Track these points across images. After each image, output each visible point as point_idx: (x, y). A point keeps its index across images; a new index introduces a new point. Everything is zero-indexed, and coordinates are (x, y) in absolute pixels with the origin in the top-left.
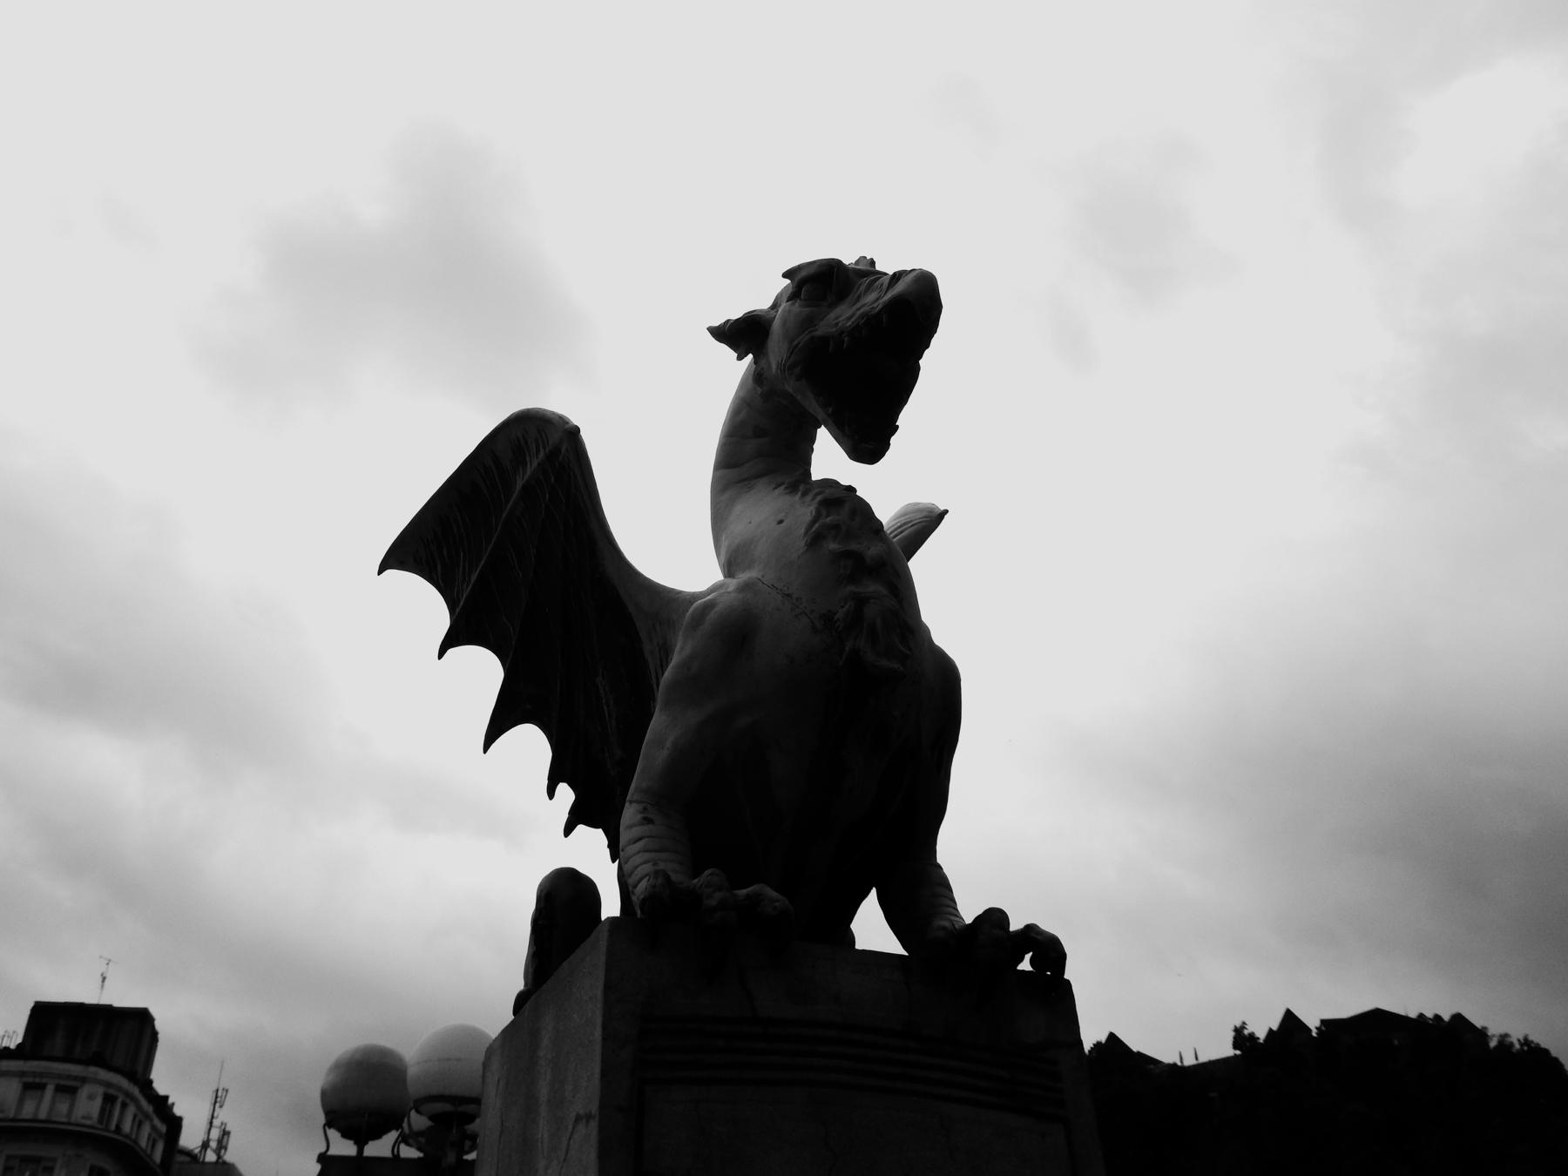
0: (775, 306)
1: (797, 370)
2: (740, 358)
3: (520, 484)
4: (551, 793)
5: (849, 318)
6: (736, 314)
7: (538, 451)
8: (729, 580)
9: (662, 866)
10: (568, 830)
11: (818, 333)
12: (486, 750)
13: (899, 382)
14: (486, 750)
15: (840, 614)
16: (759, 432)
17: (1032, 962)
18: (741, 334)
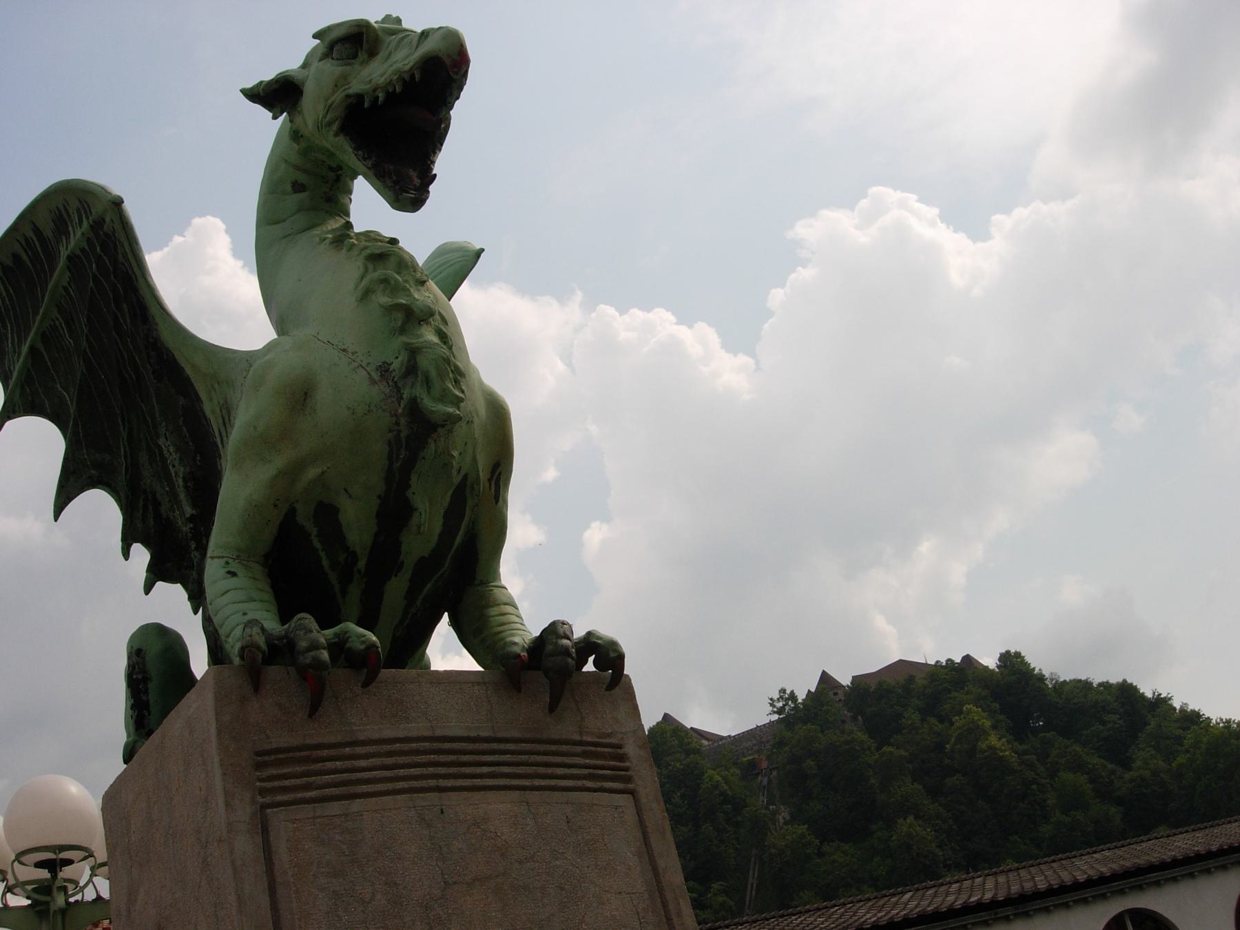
0: (305, 65)
1: (335, 127)
2: (275, 118)
3: (64, 253)
4: (126, 554)
5: (382, 76)
6: (269, 76)
7: (81, 222)
8: (285, 338)
9: (250, 616)
10: (148, 588)
11: (351, 91)
12: (56, 518)
13: (430, 135)
14: (57, 516)
15: (396, 365)
16: (298, 187)
18: (277, 95)
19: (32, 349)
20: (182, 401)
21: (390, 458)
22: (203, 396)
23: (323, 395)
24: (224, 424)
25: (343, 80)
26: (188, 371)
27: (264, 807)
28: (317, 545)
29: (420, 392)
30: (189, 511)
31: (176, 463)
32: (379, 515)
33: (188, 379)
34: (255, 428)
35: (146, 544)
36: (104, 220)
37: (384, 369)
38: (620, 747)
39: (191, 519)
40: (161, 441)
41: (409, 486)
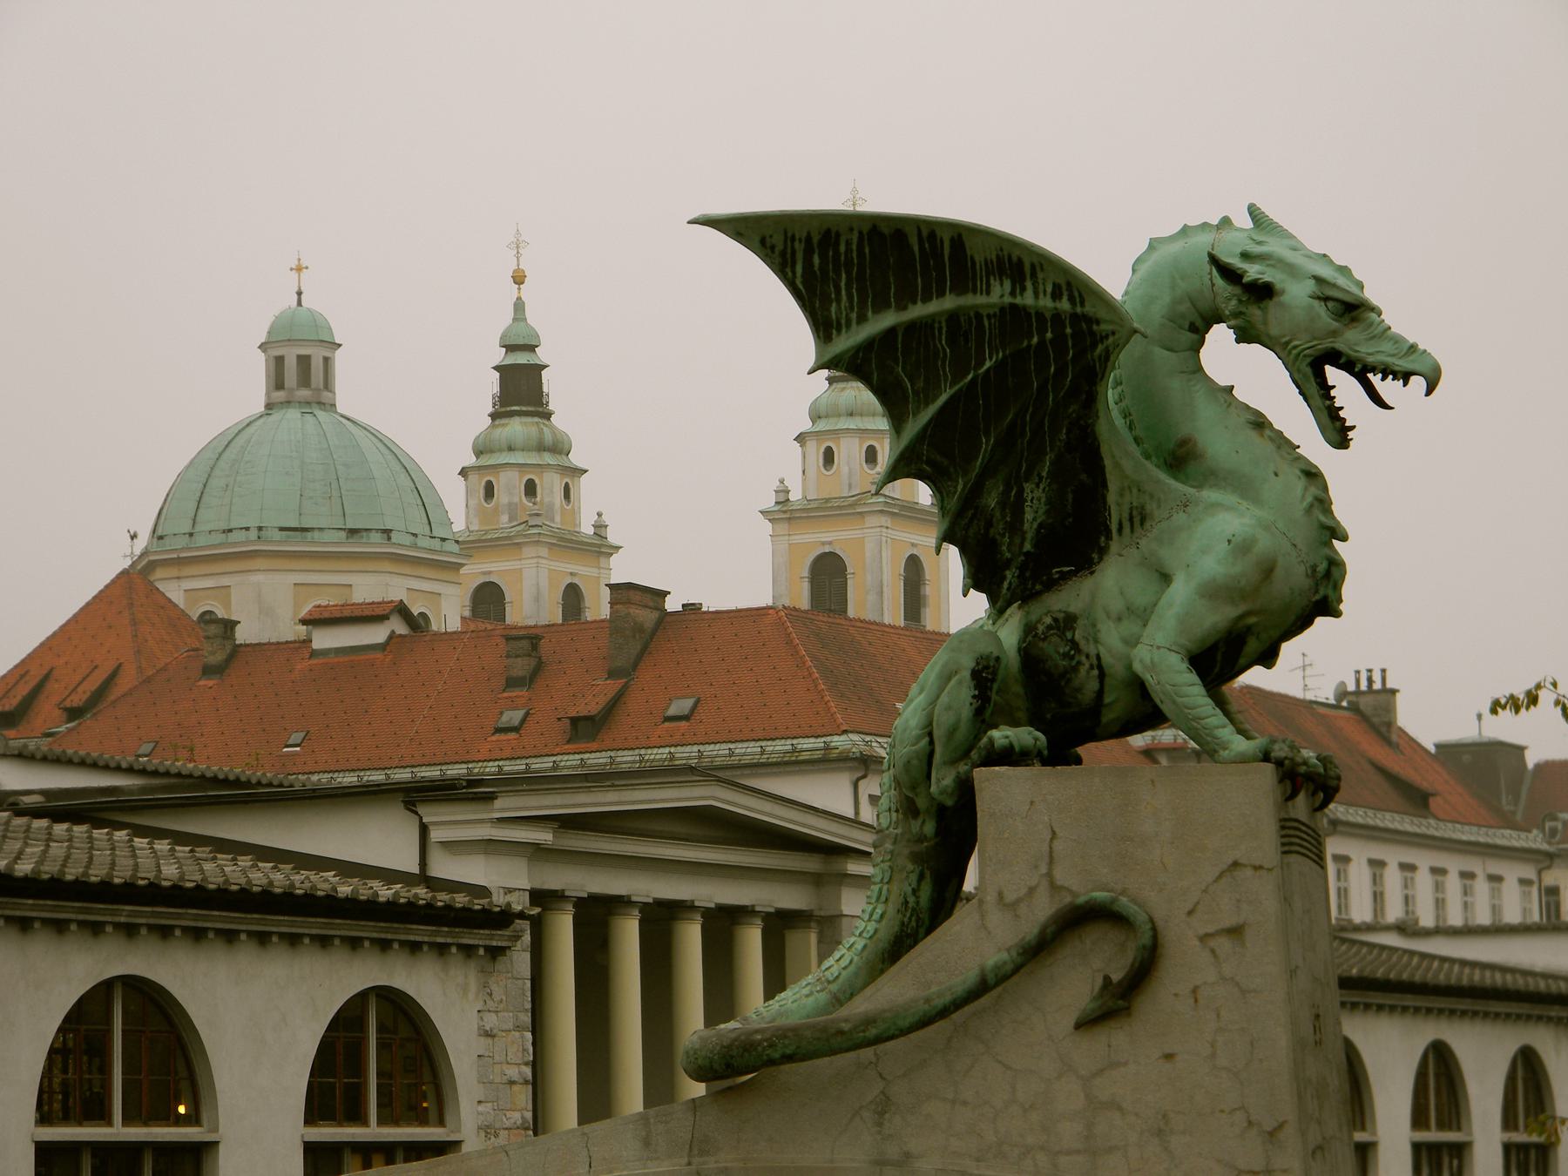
1: (1309, 360)
19: (891, 332)
20: (1084, 477)
22: (1113, 485)
23: (1279, 573)
24: (1131, 519)
25: (1334, 334)
26: (1108, 462)
29: (1330, 592)
30: (1028, 547)
31: (1041, 512)
35: (963, 552)
36: (1098, 322)
37: (1314, 568)
39: (1027, 554)
40: (1028, 487)
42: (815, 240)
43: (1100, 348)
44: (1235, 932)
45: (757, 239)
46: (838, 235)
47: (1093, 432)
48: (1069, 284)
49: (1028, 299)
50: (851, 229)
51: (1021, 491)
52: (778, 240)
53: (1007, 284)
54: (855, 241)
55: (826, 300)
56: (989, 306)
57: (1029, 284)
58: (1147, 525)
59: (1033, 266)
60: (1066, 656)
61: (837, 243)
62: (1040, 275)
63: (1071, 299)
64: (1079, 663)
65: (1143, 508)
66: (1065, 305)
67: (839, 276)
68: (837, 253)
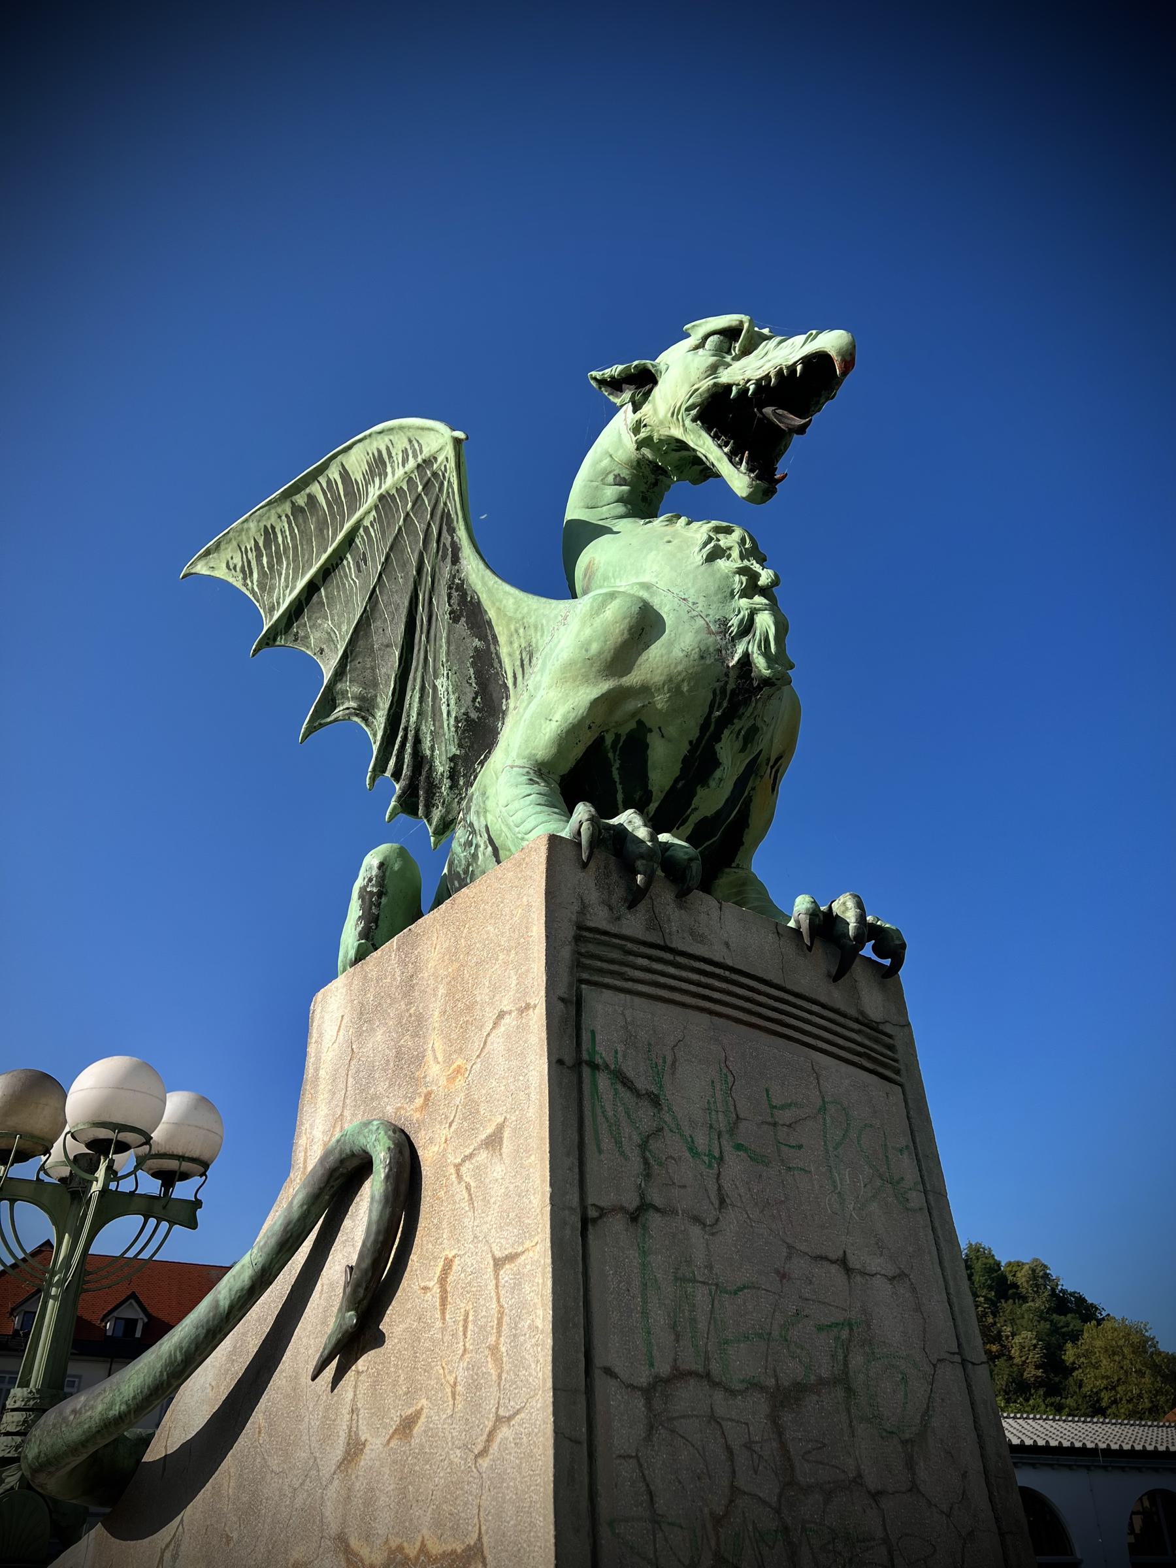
7: (405, 461)
17: (874, 948)
20: (477, 642)
21: (711, 707)
22: (502, 639)
24: (522, 665)
26: (492, 614)
27: (581, 981)
28: (616, 775)
32: (685, 761)
33: (489, 623)
34: (587, 650)
36: (436, 459)
37: (724, 623)
38: (890, 1036)
40: (438, 682)
41: (719, 740)
42: (261, 544)
43: (446, 483)
44: (494, 1142)
45: (224, 565)
46: (273, 527)
47: (469, 585)
48: (410, 441)
49: (389, 481)
50: (280, 517)
51: (435, 688)
52: (237, 560)
53: (377, 480)
54: (286, 526)
55: (272, 588)
56: (368, 512)
57: (389, 470)
58: (534, 660)
59: (388, 449)
60: (469, 843)
61: (276, 537)
62: (394, 454)
63: (415, 456)
64: (477, 846)
65: (530, 646)
66: (412, 464)
67: (280, 562)
68: (277, 546)
